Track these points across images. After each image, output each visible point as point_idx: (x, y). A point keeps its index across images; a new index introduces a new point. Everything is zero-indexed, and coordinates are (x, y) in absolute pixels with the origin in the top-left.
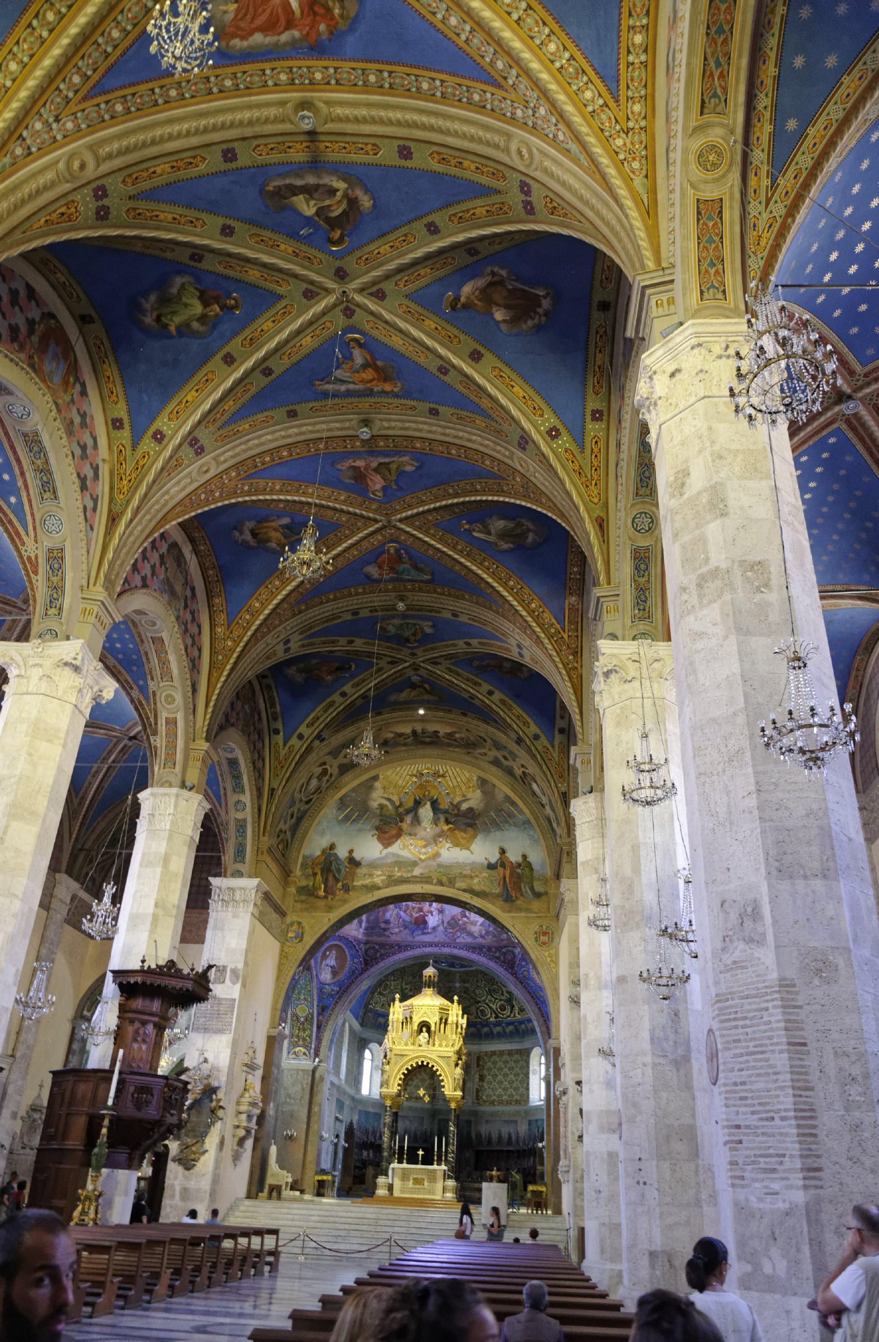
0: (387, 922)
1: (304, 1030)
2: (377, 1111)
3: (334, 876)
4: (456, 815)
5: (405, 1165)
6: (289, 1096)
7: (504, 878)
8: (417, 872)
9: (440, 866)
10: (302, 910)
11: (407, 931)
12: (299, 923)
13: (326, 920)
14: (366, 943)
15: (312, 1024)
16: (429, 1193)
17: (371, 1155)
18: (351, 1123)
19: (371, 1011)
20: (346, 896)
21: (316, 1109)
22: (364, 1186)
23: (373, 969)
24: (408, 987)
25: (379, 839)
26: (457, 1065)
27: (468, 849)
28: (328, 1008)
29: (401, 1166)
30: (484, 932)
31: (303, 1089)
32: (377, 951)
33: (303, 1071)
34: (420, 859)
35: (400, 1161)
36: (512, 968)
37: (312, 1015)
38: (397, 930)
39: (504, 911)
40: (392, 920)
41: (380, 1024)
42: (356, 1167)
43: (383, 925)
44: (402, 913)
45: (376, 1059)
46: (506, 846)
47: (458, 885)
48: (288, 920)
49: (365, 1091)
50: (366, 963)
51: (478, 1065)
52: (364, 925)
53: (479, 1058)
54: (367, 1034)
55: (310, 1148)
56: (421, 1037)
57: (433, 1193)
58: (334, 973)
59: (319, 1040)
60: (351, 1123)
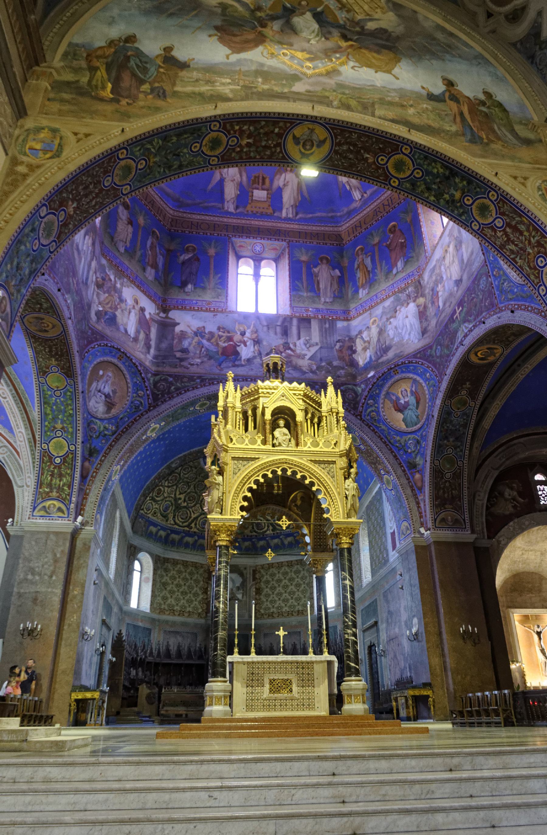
0: (185, 351)
1: (61, 476)
2: (148, 626)
3: (134, 75)
4: (358, 33)
5: (253, 657)
6: (32, 571)
7: (461, 114)
8: (299, 87)
9: (341, 86)
10: (61, 113)
11: (212, 361)
12: (54, 131)
13: (117, 131)
14: (155, 375)
15: (73, 468)
16: (302, 706)
17: (140, 674)
18: (120, 634)
19: (142, 517)
20: (160, 103)
21: (75, 591)
22: (136, 709)
23: (163, 407)
24: (182, 496)
25: (221, 40)
26: (347, 477)
27: (389, 72)
28: (98, 452)
29: (246, 658)
30: (314, 367)
31: (56, 561)
32: (171, 384)
33: (57, 534)
34: (305, 74)
35: (245, 651)
36: (355, 408)
37: (74, 453)
38: (199, 361)
39: (474, 155)
40: (191, 348)
41: (151, 533)
42: (125, 687)
43: (178, 355)
44: (205, 342)
45: (145, 571)
46: (451, 77)
47: (377, 113)
48: (29, 123)
49: (134, 604)
50: (156, 398)
51: (254, 579)
52: (152, 351)
53: (254, 571)
54: (137, 541)
55: (63, 650)
56: (277, 433)
57: (311, 707)
58: (110, 405)
59: (83, 494)
60: (120, 634)
